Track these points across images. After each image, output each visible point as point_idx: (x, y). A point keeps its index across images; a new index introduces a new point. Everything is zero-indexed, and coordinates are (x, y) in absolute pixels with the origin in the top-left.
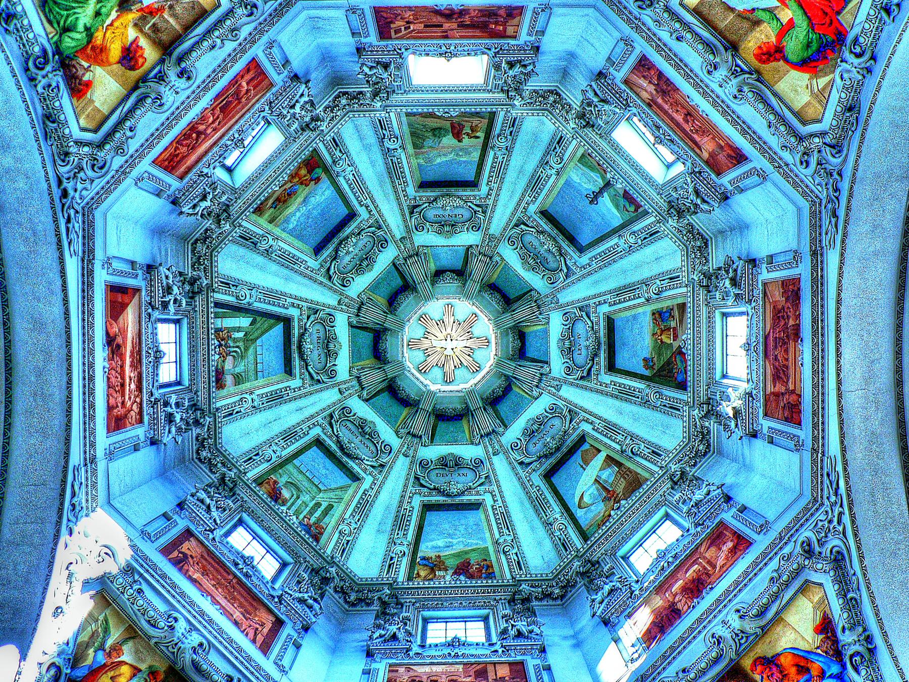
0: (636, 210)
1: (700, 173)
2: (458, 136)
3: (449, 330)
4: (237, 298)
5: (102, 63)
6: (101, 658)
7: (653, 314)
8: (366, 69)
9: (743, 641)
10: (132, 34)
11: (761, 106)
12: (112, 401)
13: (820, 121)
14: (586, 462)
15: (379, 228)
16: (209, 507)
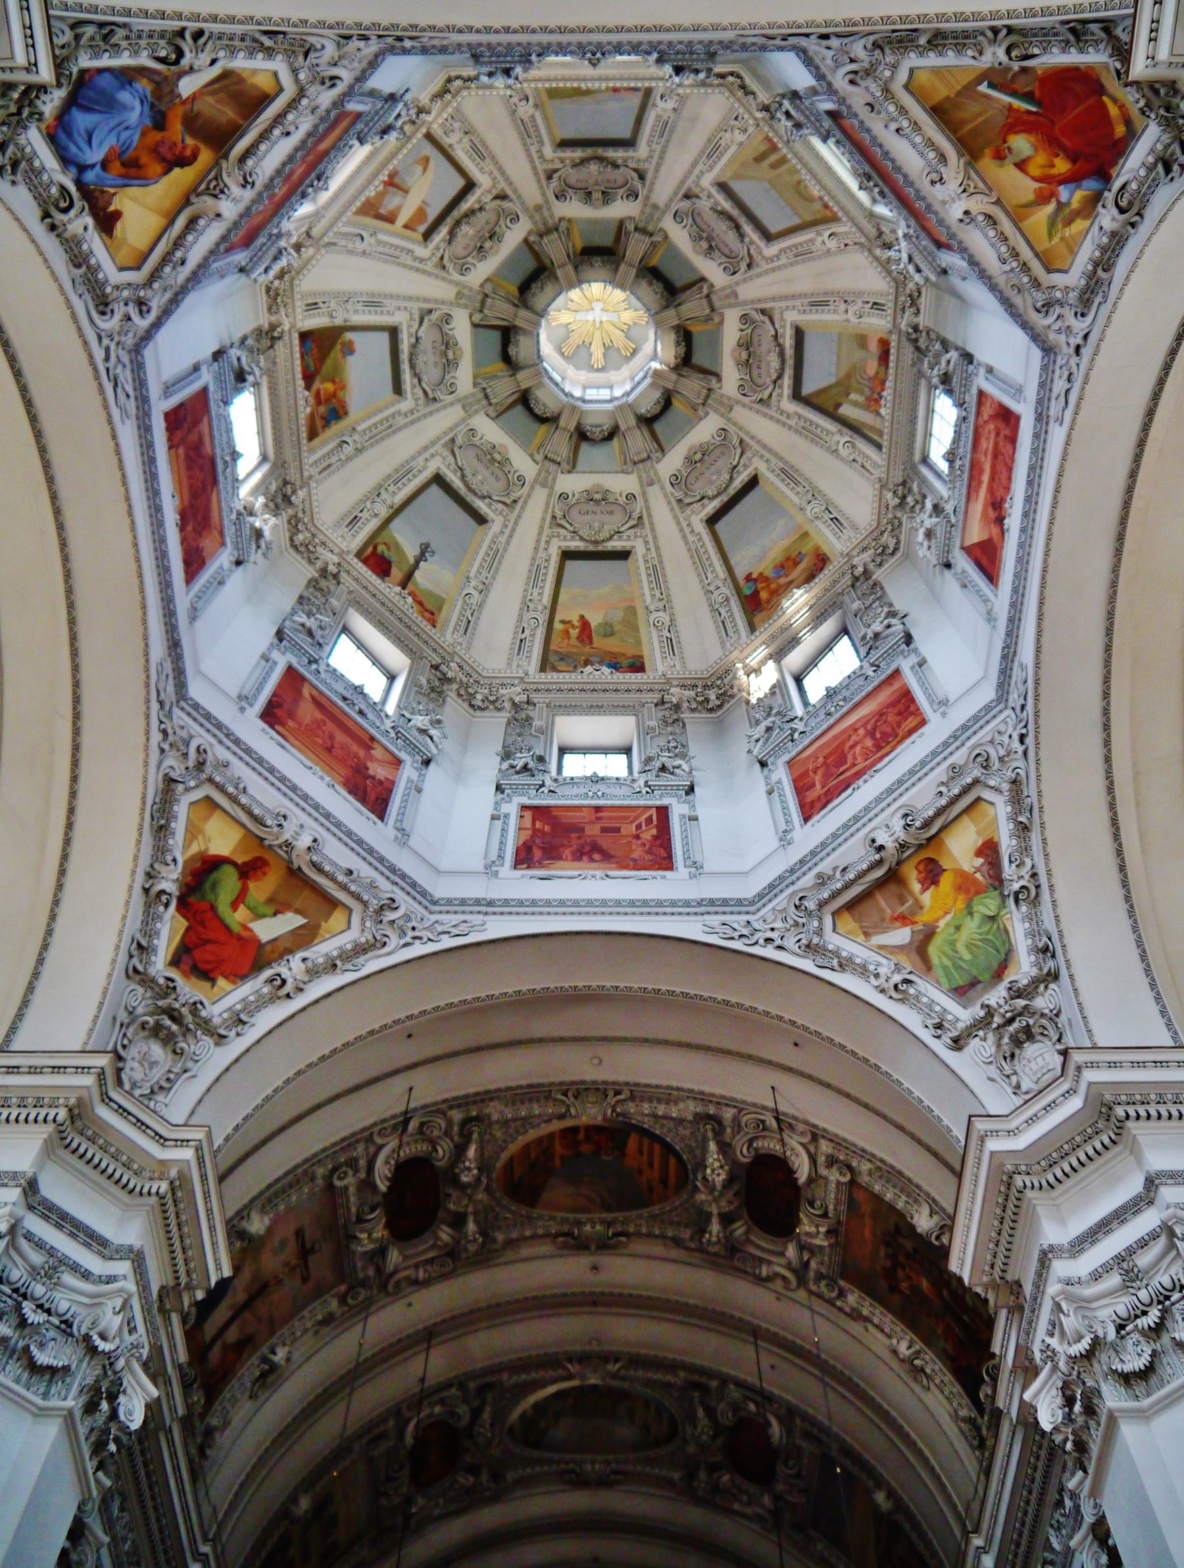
0: (375, 548)
1: (310, 662)
2: (585, 625)
3: (597, 334)
4: (854, 446)
5: (961, 874)
6: (1064, 192)
7: (346, 413)
8: (685, 767)
9: (213, 183)
10: (926, 898)
11: (257, 811)
12: (1009, 447)
13: (192, 804)
14: (420, 214)
15: (680, 501)
16: (910, 259)
